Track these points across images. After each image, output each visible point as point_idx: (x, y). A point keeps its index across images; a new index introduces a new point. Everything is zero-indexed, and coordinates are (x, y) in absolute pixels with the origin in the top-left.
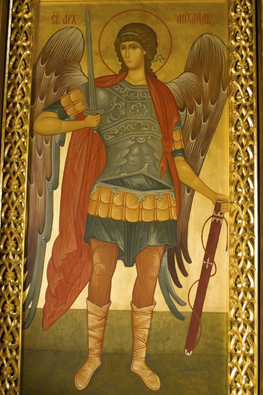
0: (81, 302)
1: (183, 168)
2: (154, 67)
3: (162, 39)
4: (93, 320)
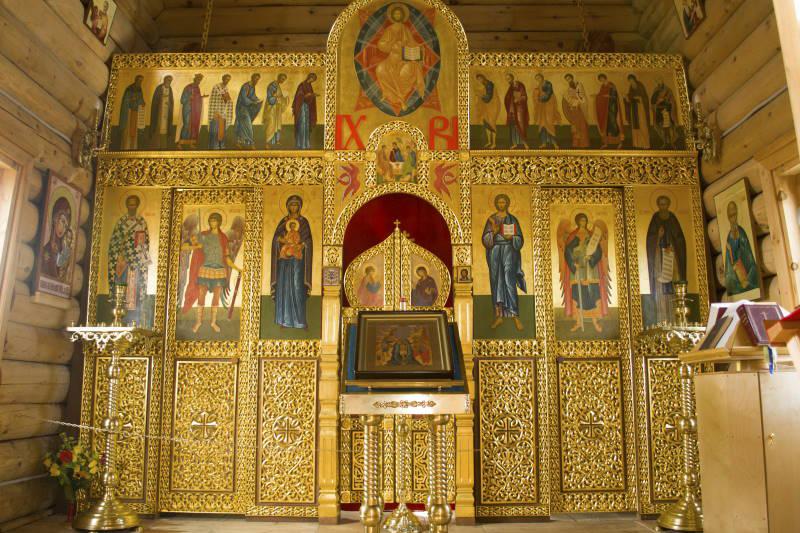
0: (195, 305)
1: (229, 261)
2: (221, 228)
3: (224, 218)
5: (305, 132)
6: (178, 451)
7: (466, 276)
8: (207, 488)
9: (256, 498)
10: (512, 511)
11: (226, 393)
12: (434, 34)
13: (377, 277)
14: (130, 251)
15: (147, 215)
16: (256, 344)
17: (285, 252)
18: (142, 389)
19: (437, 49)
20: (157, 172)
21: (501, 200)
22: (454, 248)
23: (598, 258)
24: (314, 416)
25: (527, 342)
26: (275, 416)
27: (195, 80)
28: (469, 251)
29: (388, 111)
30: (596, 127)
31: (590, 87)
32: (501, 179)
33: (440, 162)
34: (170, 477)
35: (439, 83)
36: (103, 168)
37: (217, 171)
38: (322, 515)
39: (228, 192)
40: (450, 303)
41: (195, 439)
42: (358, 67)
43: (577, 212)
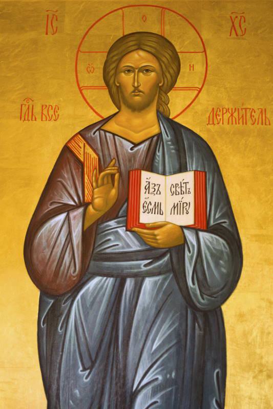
21: (138, 58)
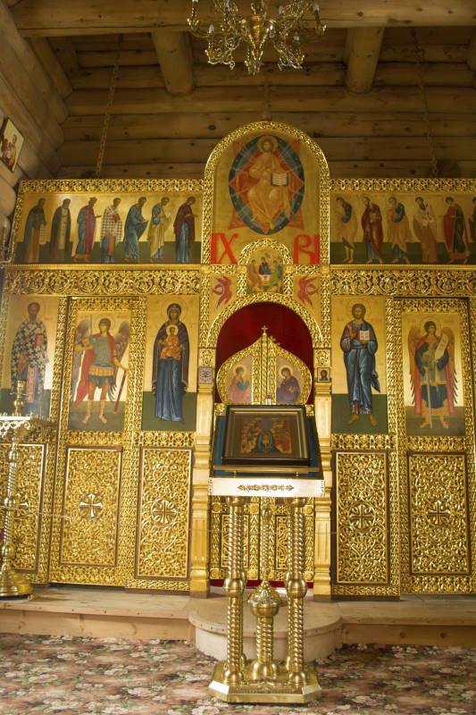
0: (86, 399)
1: (116, 361)
2: (110, 331)
3: (112, 323)
4: (89, 404)
5: (185, 249)
6: (68, 528)
7: (325, 376)
8: (92, 562)
9: (135, 572)
10: (366, 591)
11: (111, 478)
12: (299, 162)
13: (246, 376)
14: (31, 351)
15: (46, 319)
16: (138, 434)
17: (165, 353)
18: (37, 472)
19: (301, 176)
20: (55, 282)
21: (358, 309)
22: (315, 351)
23: (445, 362)
24: (188, 500)
25: (380, 437)
26: (154, 499)
27: (90, 203)
28: (328, 355)
29: (257, 230)
30: (443, 244)
31: (439, 209)
32: (357, 290)
33: (304, 275)
34: (60, 551)
35: (303, 206)
36: (8, 278)
37: (107, 281)
38: (193, 589)
39: (116, 300)
40: (311, 401)
41: (83, 517)
42: (232, 191)
43: (426, 321)
